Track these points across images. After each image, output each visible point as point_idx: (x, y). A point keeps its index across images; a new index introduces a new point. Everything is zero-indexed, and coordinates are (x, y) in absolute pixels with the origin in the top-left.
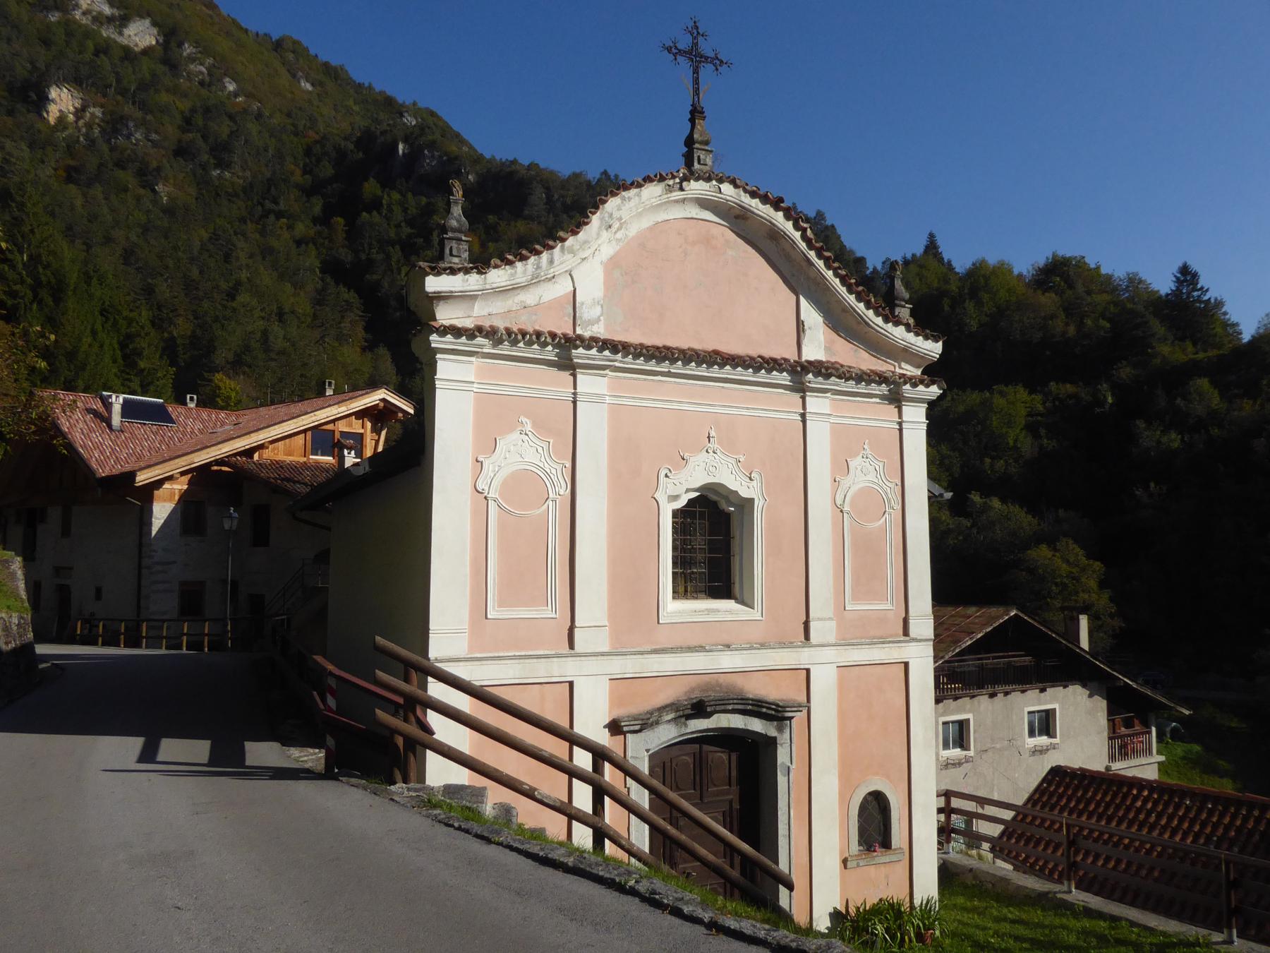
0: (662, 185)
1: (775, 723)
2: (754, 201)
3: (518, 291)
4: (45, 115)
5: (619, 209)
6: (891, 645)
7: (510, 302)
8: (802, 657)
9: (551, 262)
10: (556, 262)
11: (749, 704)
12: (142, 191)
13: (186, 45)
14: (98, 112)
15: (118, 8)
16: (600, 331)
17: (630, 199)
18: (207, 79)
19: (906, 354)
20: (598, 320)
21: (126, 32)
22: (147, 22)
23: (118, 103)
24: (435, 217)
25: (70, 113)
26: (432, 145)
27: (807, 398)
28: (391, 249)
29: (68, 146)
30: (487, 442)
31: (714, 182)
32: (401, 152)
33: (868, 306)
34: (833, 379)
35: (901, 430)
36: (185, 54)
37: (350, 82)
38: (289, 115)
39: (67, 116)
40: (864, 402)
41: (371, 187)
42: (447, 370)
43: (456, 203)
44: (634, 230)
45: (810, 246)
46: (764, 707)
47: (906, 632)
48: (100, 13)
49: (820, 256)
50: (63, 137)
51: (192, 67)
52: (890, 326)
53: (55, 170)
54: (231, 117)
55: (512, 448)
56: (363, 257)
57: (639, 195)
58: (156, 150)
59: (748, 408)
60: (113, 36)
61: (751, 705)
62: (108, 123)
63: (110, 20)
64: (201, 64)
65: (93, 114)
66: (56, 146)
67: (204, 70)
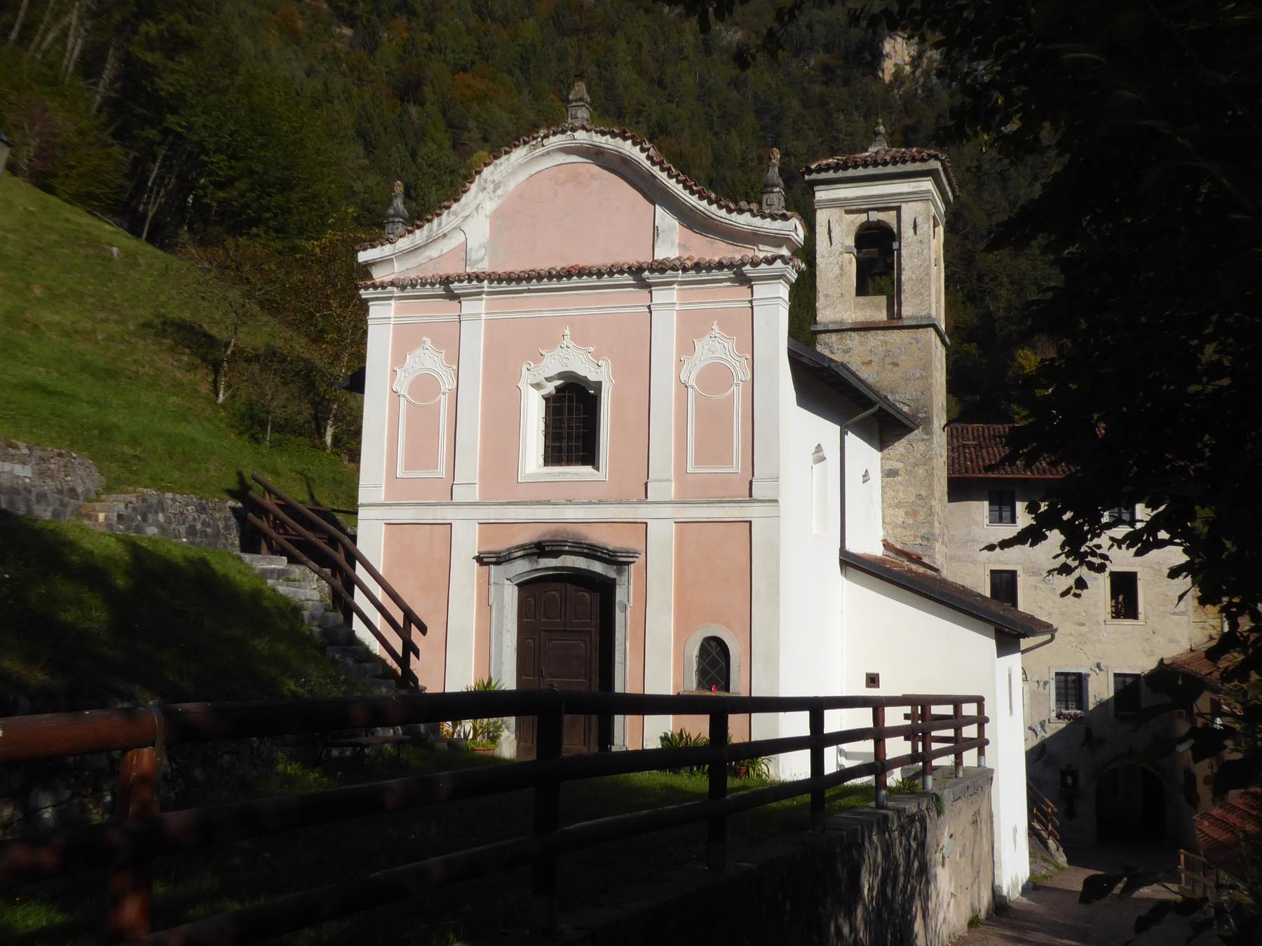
0: (527, 147)
1: (615, 567)
3: (423, 249)
4: (881, 74)
5: (492, 173)
6: (731, 505)
7: (420, 258)
8: (640, 513)
9: (440, 224)
16: (484, 267)
17: (501, 164)
19: (754, 238)
20: (483, 259)
25: (907, 64)
29: (905, 104)
30: (399, 359)
31: (569, 133)
33: (711, 202)
34: (669, 272)
35: (752, 307)
39: (904, 69)
42: (375, 311)
43: (396, 197)
44: (512, 185)
45: (654, 163)
46: (565, 546)
47: (751, 495)
49: (662, 170)
50: (900, 96)
55: (417, 360)
59: (598, 308)
65: (931, 60)
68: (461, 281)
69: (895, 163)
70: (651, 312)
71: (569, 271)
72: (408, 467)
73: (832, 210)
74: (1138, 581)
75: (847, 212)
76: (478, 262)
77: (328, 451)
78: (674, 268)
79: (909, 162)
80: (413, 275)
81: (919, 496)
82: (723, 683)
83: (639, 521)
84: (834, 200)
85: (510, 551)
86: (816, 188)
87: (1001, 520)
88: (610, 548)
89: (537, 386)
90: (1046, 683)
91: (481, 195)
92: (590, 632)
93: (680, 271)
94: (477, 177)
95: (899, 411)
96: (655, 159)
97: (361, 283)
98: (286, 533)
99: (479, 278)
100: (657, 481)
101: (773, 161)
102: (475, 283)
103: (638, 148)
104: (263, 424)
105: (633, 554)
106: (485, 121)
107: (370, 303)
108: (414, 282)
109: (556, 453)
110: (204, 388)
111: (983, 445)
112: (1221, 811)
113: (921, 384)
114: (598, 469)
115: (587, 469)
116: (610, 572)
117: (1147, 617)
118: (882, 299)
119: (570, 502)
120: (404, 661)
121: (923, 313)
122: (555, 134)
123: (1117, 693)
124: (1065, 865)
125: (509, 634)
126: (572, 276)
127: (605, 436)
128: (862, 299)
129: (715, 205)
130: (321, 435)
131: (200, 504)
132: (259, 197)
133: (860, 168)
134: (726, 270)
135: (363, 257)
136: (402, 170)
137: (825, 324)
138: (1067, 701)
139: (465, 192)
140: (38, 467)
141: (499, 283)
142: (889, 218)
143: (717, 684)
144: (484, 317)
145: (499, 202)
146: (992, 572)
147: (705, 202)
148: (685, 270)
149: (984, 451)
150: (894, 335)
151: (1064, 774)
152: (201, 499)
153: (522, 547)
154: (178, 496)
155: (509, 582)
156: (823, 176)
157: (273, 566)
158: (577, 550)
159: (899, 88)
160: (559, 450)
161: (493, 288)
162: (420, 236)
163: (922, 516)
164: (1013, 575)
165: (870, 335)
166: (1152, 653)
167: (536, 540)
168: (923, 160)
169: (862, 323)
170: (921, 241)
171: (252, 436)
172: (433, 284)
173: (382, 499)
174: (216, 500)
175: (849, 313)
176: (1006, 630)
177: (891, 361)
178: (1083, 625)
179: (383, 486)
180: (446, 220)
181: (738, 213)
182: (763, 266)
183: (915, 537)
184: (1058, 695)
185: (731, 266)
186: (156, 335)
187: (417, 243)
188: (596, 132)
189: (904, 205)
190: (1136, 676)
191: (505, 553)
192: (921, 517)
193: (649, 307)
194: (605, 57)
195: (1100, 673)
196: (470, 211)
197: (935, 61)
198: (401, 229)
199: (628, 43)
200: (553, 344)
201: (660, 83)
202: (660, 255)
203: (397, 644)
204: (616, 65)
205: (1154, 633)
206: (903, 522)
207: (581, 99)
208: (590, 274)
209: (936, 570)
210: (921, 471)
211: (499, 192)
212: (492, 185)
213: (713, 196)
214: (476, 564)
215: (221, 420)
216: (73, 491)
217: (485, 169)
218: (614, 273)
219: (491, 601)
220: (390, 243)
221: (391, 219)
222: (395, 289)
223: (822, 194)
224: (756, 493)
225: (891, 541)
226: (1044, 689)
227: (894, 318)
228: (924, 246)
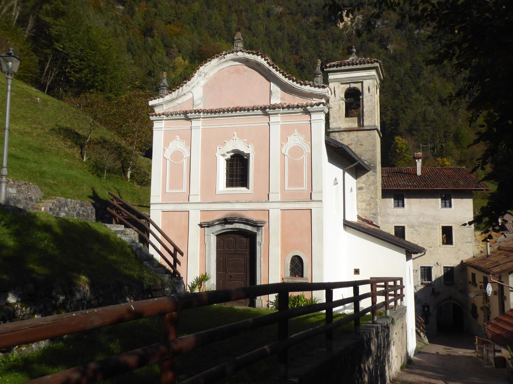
0: (218, 58)
1: (256, 228)
3: (175, 100)
4: (338, 25)
5: (204, 69)
6: (303, 203)
8: (266, 206)
9: (182, 90)
11: (244, 220)
12: (381, 50)
14: (360, 17)
16: (201, 107)
17: (207, 65)
19: (311, 95)
20: (200, 104)
23: (369, 10)
27: (270, 117)
30: (166, 144)
31: (235, 53)
33: (293, 81)
34: (277, 109)
35: (311, 123)
39: (348, 23)
42: (156, 125)
43: (164, 79)
44: (212, 74)
45: (270, 65)
46: (236, 220)
47: (311, 199)
49: (274, 68)
50: (346, 34)
52: (303, 86)
53: (343, 50)
55: (174, 145)
57: (210, 64)
58: (387, 28)
59: (248, 124)
61: (237, 220)
62: (365, 21)
65: (358, 19)
66: (343, 39)
68: (191, 113)
69: (361, 64)
71: (236, 109)
72: (170, 188)
73: (336, 83)
74: (453, 230)
75: (341, 84)
76: (198, 105)
78: (279, 108)
80: (171, 110)
81: (372, 198)
82: (301, 274)
83: (266, 209)
84: (336, 79)
85: (213, 222)
86: (329, 74)
87: (398, 206)
88: (254, 220)
89: (223, 155)
90: (417, 271)
91: (199, 78)
92: (246, 254)
93: (281, 109)
94: (198, 70)
95: (365, 164)
96: (270, 63)
97: (150, 114)
98: (123, 215)
99: (199, 112)
100: (273, 193)
101: (318, 64)
102: (197, 114)
103: (263, 59)
104: (102, 170)
105: (263, 223)
106: (180, 44)
107: (154, 122)
108: (172, 113)
109: (230, 183)
110: (78, 156)
111: (390, 176)
112: (495, 321)
113: (372, 153)
114: (249, 189)
115: (244, 189)
116: (254, 230)
117: (456, 244)
118: (356, 119)
119: (237, 202)
120: (174, 267)
121: (373, 124)
122: (229, 53)
123: (445, 274)
124: (428, 343)
125: (213, 255)
126: (237, 111)
128: (348, 119)
129: (295, 82)
130: (126, 175)
131: (81, 203)
132: (94, 76)
133: (347, 66)
134: (300, 108)
135: (151, 103)
136: (147, 65)
137: (333, 129)
138: (425, 278)
139: (192, 77)
140: (17, 189)
141: (207, 114)
142: (358, 86)
143: (298, 274)
144: (201, 127)
145: (207, 81)
146: (395, 227)
148: (283, 108)
149: (391, 178)
150: (361, 133)
151: (424, 307)
152: (82, 201)
153: (218, 220)
154: (73, 200)
155: (213, 234)
156: (332, 69)
157: (119, 229)
158: (241, 221)
159: (346, 31)
161: (205, 116)
162: (174, 94)
163: (373, 205)
164: (403, 228)
165: (351, 133)
166: (458, 258)
167: (224, 218)
168: (372, 63)
169: (348, 128)
170: (371, 95)
171: (98, 175)
172: (180, 114)
173: (160, 202)
174: (88, 201)
175: (342, 124)
176: (410, 251)
177: (360, 143)
178: (431, 247)
179: (161, 196)
180: (185, 88)
181: (305, 85)
182: (315, 107)
184: (421, 275)
185: (302, 107)
186: (56, 133)
188: (246, 53)
189: (364, 81)
190: (452, 268)
192: (372, 206)
193: (269, 123)
194: (227, 18)
195: (438, 267)
197: (360, 20)
198: (166, 92)
200: (229, 138)
201: (250, 29)
202: (273, 102)
203: (171, 260)
204: (232, 21)
205: (459, 250)
206: (365, 208)
207: (240, 39)
208: (245, 110)
209: (379, 227)
210: (372, 188)
211: (206, 77)
213: (294, 78)
214: (199, 227)
215: (85, 169)
216: (31, 198)
217: (201, 67)
218: (254, 110)
220: (162, 97)
221: (162, 88)
222: (164, 116)
223: (331, 77)
225: (361, 215)
226: (416, 273)
227: (361, 126)
228: (373, 97)
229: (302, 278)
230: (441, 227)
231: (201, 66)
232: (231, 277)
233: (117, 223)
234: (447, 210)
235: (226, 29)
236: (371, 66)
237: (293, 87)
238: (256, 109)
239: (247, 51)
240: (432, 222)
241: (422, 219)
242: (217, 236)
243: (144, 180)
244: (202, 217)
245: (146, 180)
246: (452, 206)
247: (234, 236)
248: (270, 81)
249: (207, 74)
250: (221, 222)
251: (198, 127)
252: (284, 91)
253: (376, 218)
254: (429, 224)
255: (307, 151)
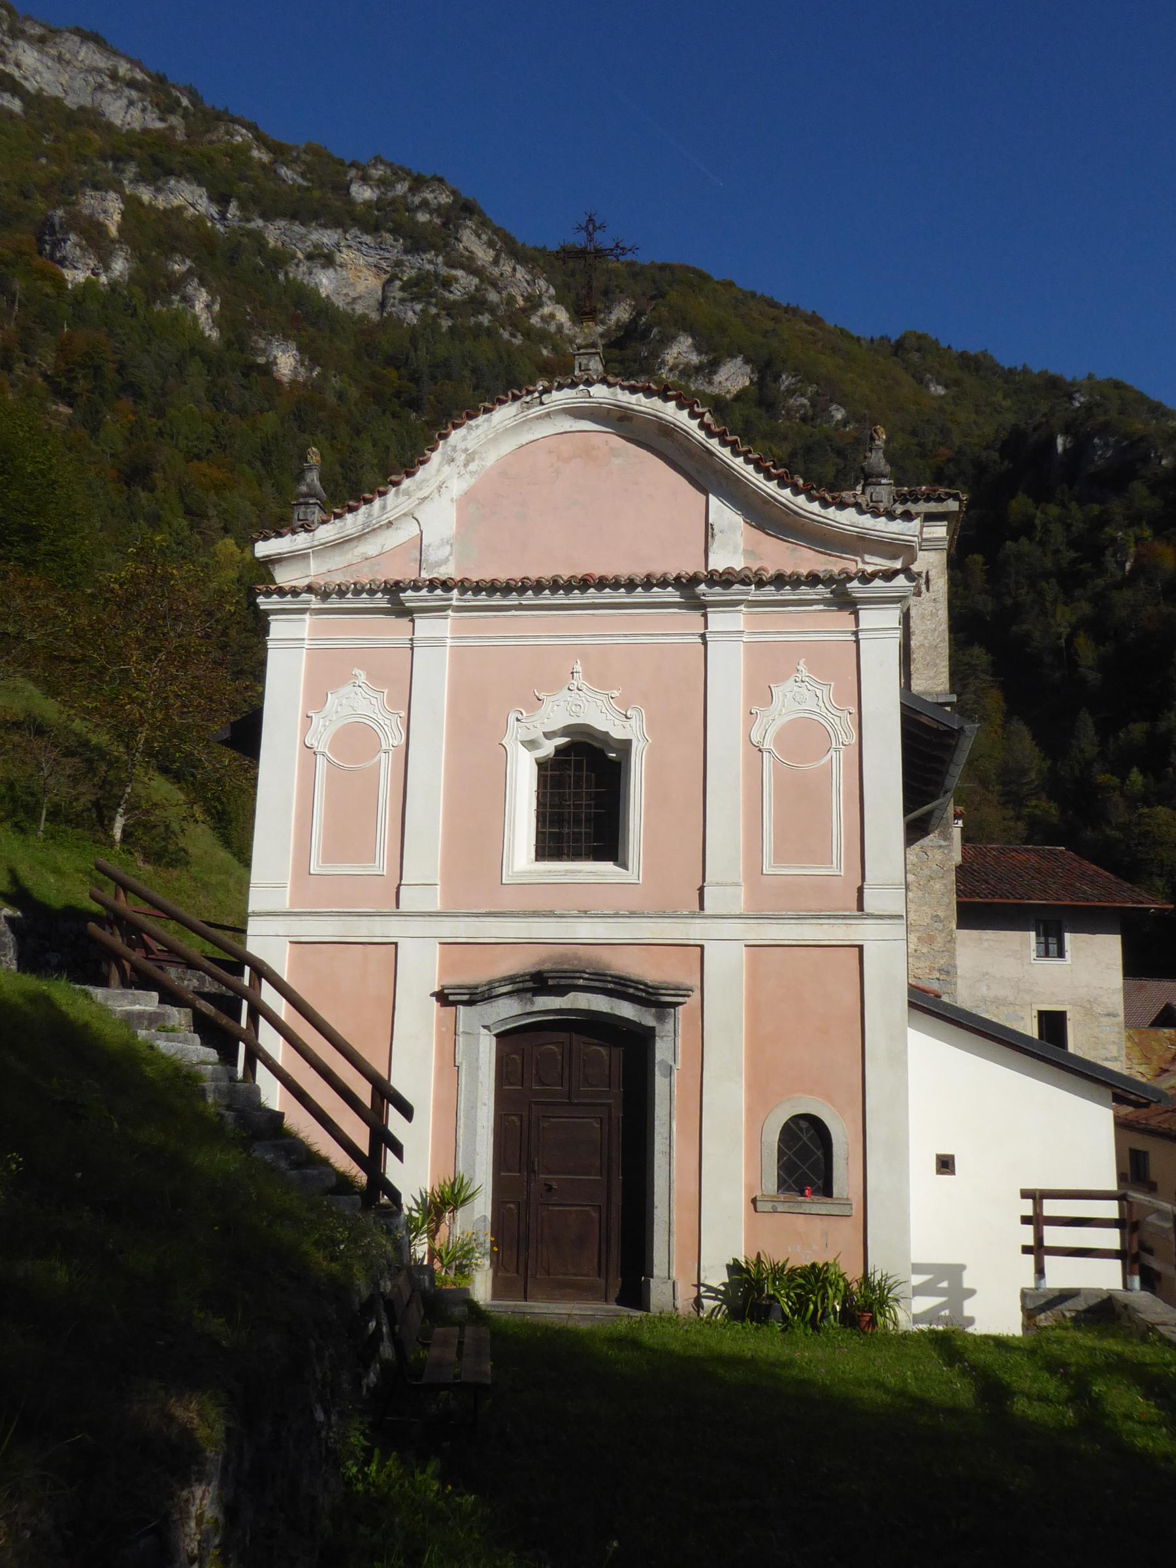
0: (518, 403)
1: (653, 1010)
2: (636, 396)
3: (354, 543)
5: (464, 439)
6: (832, 921)
8: (693, 930)
9: (384, 507)
10: (389, 508)
11: (610, 982)
13: (784, 377)
15: (706, 353)
17: (477, 426)
18: (810, 413)
19: (860, 544)
20: (446, 561)
21: (717, 379)
22: (739, 361)
24: (1107, 529)
26: (1105, 429)
27: (709, 615)
28: (1043, 584)
30: (316, 698)
31: (581, 387)
32: (1060, 449)
33: (797, 491)
34: (736, 586)
35: (857, 642)
36: (782, 388)
37: (995, 369)
38: (914, 433)
40: (779, 612)
41: (1020, 505)
42: (278, 628)
43: (310, 469)
44: (491, 458)
45: (710, 434)
47: (860, 907)
48: (687, 365)
49: (724, 443)
51: (792, 401)
52: (832, 512)
54: (840, 453)
55: (344, 701)
56: (1009, 601)
57: (488, 420)
59: (625, 636)
60: (702, 388)
63: (698, 369)
64: (802, 395)
67: (805, 401)
68: (416, 587)
70: (705, 643)
72: (327, 858)
76: (439, 564)
77: (117, 848)
78: (745, 581)
79: (922, 502)
80: (338, 579)
82: (820, 1183)
83: (692, 942)
85: (491, 985)
88: (650, 983)
89: (531, 744)
91: (446, 469)
92: (609, 1105)
93: (753, 587)
94: (441, 442)
96: (713, 427)
98: (148, 950)
99: (446, 585)
100: (718, 884)
101: (877, 442)
102: (439, 592)
103: (685, 412)
105: (682, 991)
106: (226, 511)
107: (272, 617)
108: (343, 588)
114: (625, 866)
115: (607, 867)
119: (585, 914)
120: (372, 1163)
122: (560, 387)
125: (485, 1109)
126: (589, 587)
127: (637, 818)
130: (107, 827)
135: (263, 549)
139: (423, 463)
147: (787, 492)
148: (760, 584)
153: (511, 980)
155: (486, 1031)
157: (137, 1007)
158: (597, 984)
160: (558, 837)
161: (465, 600)
162: (352, 523)
167: (533, 970)
168: (940, 500)
171: (16, 825)
172: (372, 592)
173: (286, 906)
176: (1132, 1097)
179: (288, 885)
180: (394, 502)
181: (837, 509)
183: (932, 969)
185: (829, 581)
187: (348, 532)
188: (623, 388)
191: (485, 988)
193: (703, 636)
194: (350, 457)
196: (430, 491)
198: (317, 514)
199: (374, 446)
200: (555, 685)
202: (719, 562)
203: (360, 1136)
204: (361, 467)
206: (916, 951)
210: (937, 887)
211: (472, 467)
212: (463, 456)
213: (801, 482)
214: (434, 1004)
217: (453, 432)
219: (459, 1059)
220: (307, 531)
221: (301, 500)
222: (313, 597)
224: (870, 905)
229: (828, 1200)
230: (1035, 1013)
231: (456, 426)
232: (550, 1189)
233: (126, 984)
234: (1052, 963)
235: (347, 484)
236: (935, 511)
237: (796, 513)
238: (657, 585)
239: (625, 383)
240: (1011, 998)
241: (984, 990)
242: (501, 1037)
243: (165, 849)
244: (444, 970)
245: (171, 848)
246: (1067, 955)
247: (563, 1036)
248: (706, 493)
249: (477, 456)
250: (521, 985)
251: (438, 642)
252: (760, 527)
253: (950, 983)
254: (1004, 1005)
255: (842, 737)
